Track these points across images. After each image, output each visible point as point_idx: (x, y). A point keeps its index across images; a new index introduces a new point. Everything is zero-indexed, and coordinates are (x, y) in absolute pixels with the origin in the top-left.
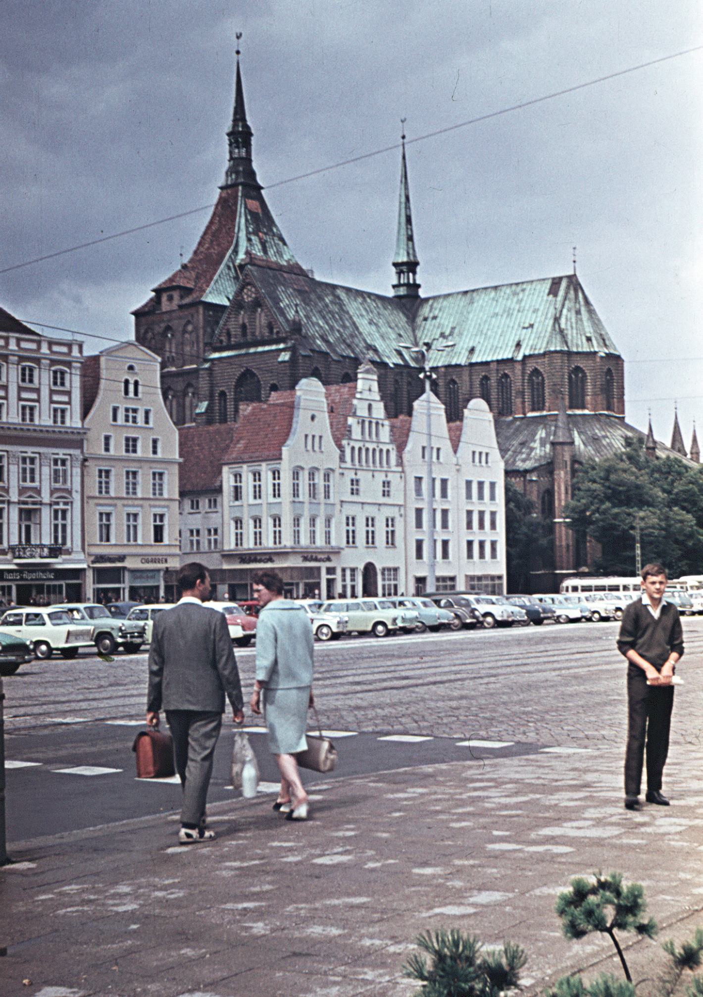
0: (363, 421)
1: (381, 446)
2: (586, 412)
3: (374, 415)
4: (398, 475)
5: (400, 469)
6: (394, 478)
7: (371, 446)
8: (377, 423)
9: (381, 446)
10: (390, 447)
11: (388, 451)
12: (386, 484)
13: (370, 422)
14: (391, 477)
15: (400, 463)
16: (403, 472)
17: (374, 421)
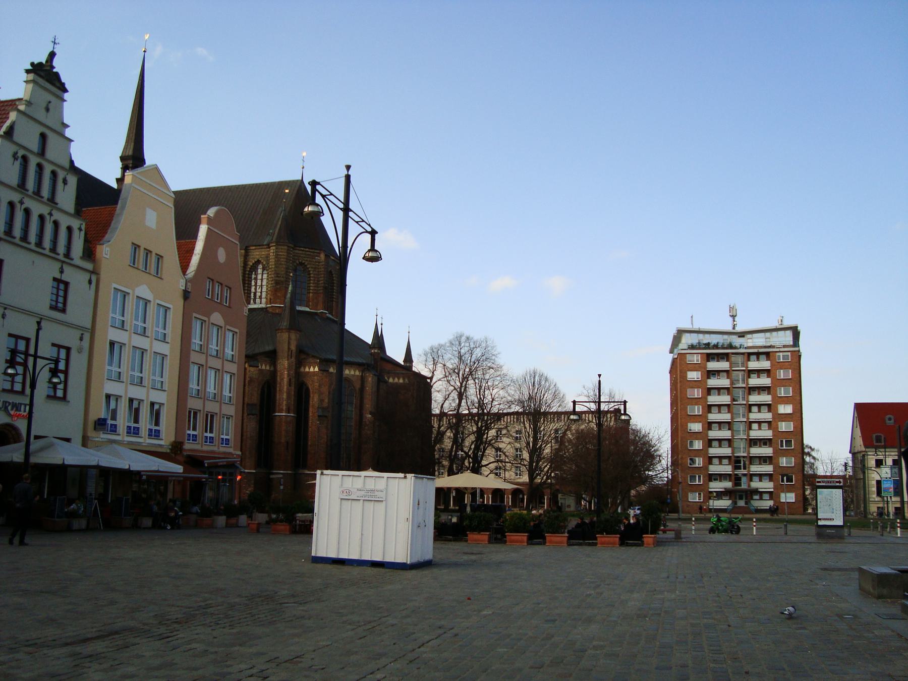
0: (25, 159)
1: (57, 216)
2: (308, 309)
3: (49, 154)
4: (87, 276)
5: (89, 266)
6: (77, 280)
7: (37, 209)
8: (54, 173)
9: (57, 216)
10: (76, 223)
11: (69, 229)
12: (63, 287)
13: (40, 167)
14: (69, 275)
15: (89, 254)
16: (95, 272)
17: (48, 169)
